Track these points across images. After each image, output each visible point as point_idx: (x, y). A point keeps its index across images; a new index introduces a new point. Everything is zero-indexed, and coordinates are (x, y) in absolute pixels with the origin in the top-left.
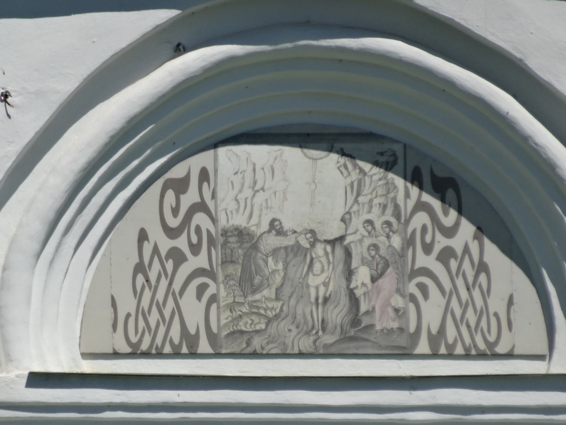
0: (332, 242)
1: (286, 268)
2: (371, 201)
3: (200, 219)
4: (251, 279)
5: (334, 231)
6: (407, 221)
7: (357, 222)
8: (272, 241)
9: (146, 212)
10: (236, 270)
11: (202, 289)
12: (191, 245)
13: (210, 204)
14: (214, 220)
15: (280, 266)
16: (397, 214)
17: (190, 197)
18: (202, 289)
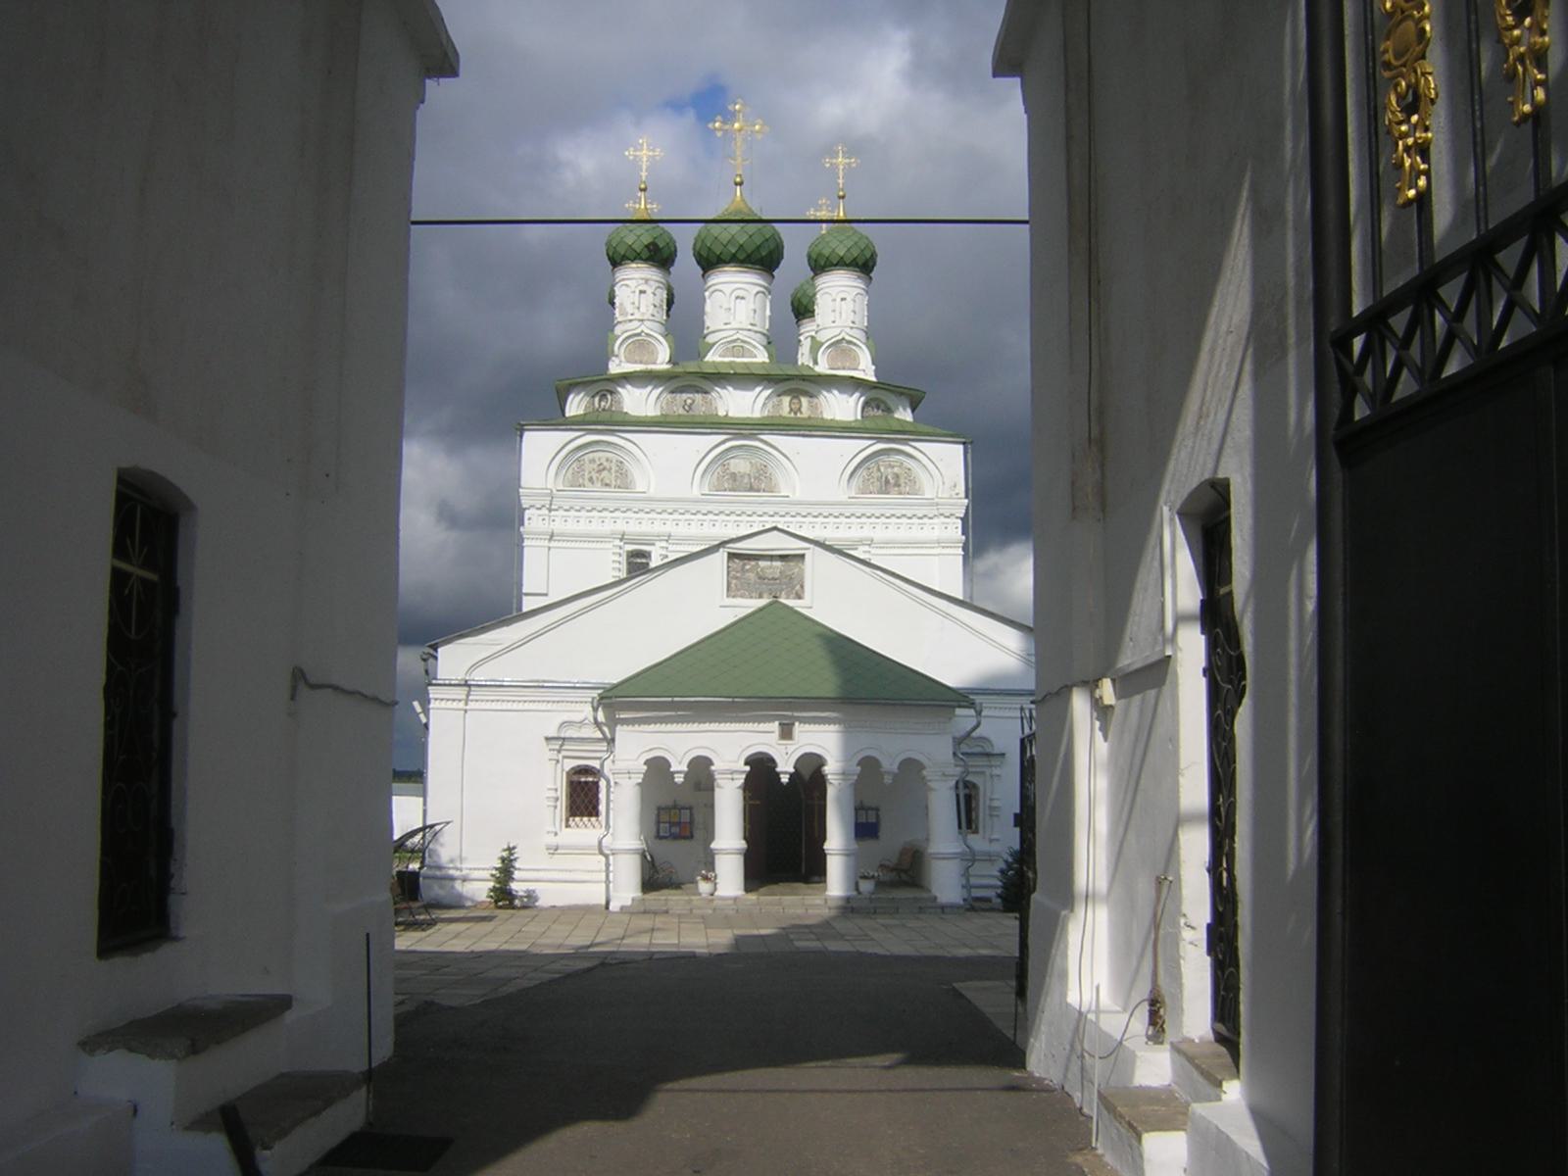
9: (719, 470)
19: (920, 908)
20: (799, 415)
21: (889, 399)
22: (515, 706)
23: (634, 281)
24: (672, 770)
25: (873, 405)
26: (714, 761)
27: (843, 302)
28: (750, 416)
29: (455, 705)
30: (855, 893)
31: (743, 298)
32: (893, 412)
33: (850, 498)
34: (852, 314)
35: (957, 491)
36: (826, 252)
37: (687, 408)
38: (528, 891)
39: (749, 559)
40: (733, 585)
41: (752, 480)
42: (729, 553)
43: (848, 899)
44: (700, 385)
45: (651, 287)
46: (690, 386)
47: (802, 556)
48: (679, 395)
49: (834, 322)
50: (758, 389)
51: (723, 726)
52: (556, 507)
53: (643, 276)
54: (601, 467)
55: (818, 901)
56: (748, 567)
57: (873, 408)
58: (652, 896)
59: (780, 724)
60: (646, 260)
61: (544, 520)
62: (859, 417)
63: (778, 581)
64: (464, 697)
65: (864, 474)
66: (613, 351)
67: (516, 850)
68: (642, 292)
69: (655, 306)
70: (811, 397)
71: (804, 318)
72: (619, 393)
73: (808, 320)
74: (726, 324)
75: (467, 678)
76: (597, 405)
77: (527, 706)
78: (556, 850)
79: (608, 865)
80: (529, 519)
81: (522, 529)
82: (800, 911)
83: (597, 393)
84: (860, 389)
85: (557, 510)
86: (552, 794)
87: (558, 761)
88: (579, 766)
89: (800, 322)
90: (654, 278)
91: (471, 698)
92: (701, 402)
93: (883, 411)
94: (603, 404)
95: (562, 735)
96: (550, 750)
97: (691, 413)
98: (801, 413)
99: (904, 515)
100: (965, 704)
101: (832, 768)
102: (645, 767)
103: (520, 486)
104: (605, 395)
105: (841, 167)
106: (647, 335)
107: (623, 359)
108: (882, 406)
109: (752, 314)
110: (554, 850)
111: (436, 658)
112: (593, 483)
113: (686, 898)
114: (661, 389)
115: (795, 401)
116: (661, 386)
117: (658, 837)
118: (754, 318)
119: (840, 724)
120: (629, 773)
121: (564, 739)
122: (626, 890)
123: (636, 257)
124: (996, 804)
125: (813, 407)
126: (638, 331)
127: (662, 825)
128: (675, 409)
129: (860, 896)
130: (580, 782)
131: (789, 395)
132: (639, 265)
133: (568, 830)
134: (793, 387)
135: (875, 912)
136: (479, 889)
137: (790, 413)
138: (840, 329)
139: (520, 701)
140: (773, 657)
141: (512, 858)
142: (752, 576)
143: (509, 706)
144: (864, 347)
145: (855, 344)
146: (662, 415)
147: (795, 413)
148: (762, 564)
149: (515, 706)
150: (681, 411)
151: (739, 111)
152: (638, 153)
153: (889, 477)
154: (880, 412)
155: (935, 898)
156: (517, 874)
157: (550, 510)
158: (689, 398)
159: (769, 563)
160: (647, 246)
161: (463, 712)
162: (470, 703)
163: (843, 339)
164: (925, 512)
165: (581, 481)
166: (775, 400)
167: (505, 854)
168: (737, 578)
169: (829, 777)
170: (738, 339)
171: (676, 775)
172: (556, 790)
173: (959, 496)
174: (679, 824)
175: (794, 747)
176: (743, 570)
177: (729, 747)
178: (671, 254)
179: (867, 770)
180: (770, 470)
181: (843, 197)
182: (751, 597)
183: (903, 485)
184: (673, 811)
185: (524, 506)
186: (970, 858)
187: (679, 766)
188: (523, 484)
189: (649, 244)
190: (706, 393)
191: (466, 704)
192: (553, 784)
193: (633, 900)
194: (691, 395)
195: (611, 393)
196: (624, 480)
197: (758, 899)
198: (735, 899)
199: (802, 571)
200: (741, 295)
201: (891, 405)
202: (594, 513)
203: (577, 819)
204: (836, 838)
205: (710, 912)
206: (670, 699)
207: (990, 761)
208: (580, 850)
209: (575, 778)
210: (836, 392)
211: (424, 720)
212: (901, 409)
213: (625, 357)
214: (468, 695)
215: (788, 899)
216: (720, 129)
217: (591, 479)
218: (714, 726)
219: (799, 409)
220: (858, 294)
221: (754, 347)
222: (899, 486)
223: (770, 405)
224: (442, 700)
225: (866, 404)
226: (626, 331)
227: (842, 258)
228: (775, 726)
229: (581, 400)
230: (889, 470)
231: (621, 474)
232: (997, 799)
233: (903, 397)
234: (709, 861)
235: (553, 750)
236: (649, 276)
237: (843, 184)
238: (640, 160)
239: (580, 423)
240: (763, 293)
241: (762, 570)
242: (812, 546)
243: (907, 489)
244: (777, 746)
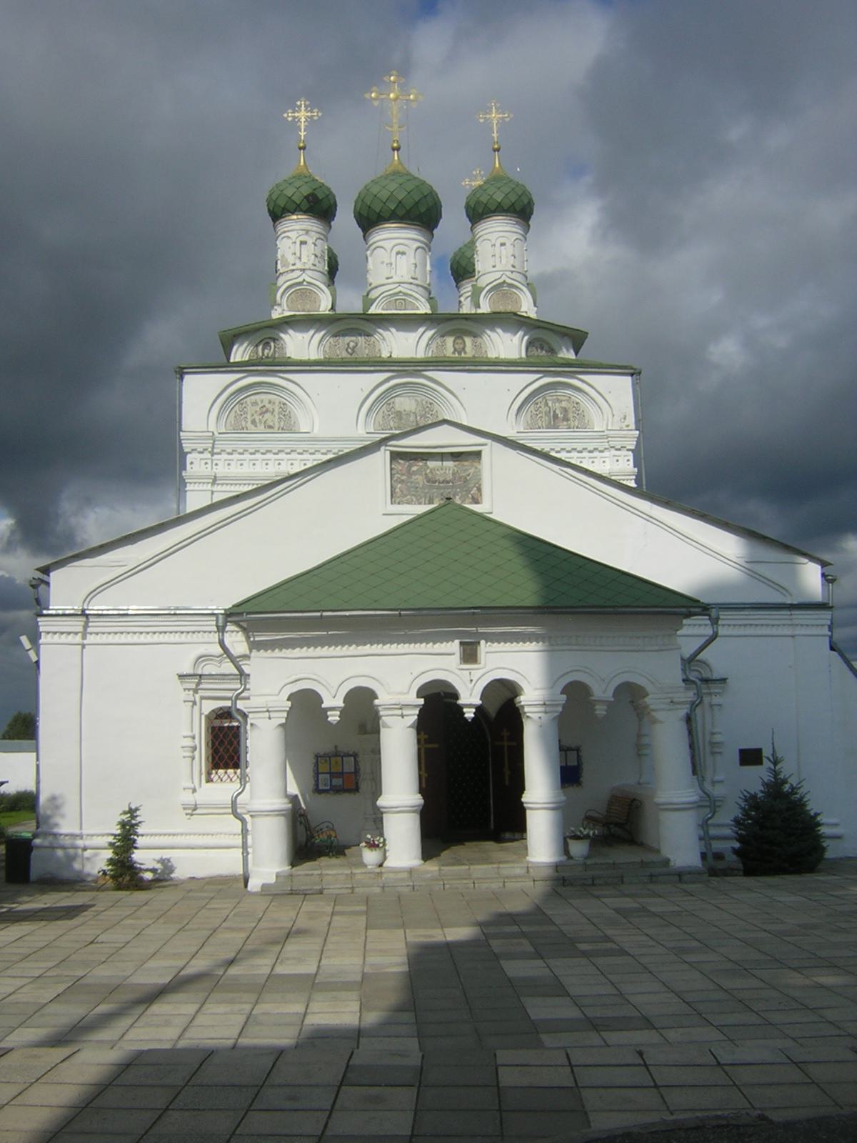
7: (418, 410)
8: (404, 413)
17: (391, 406)
19: (651, 876)
20: (463, 355)
22: (143, 639)
23: (295, 232)
24: (323, 706)
25: (537, 344)
26: (378, 693)
27: (503, 247)
28: (414, 356)
29: (70, 639)
30: (564, 858)
31: (403, 253)
32: (556, 353)
33: (518, 432)
34: (513, 258)
35: (626, 423)
36: (484, 199)
37: (349, 350)
38: (162, 861)
40: (397, 490)
41: (418, 418)
42: (392, 453)
43: (557, 867)
44: (362, 328)
45: (312, 237)
48: (341, 338)
49: (494, 267)
50: (421, 330)
51: (388, 648)
52: (219, 451)
53: (303, 227)
54: (264, 409)
55: (518, 870)
56: (414, 468)
58: (306, 868)
59: (461, 643)
60: (305, 212)
61: (206, 463)
62: (524, 355)
63: (451, 484)
64: (81, 629)
65: (532, 408)
66: (275, 301)
67: (138, 813)
68: (303, 243)
69: (316, 256)
70: (475, 337)
71: (463, 280)
72: (281, 338)
73: (467, 281)
74: (387, 278)
75: (85, 607)
76: (260, 354)
77: (156, 638)
78: (195, 809)
79: (245, 832)
80: (192, 463)
81: (184, 474)
82: (495, 886)
83: (261, 341)
84: (524, 328)
85: (219, 454)
86: (188, 742)
87: (194, 703)
88: (221, 708)
89: (459, 285)
90: (315, 229)
91: (89, 630)
93: (546, 351)
94: (266, 351)
95: (200, 672)
96: (185, 689)
97: (354, 355)
98: (465, 353)
99: (575, 449)
100: (696, 610)
101: (532, 697)
102: (289, 704)
103: (180, 430)
105: (495, 122)
106: (310, 283)
107: (286, 308)
108: (546, 347)
109: (413, 269)
110: (193, 809)
111: (48, 584)
112: (256, 426)
113: (348, 872)
116: (323, 330)
117: (317, 790)
118: (415, 272)
119: (543, 642)
120: (268, 711)
121: (200, 676)
122: (269, 862)
123: (297, 209)
124: (718, 738)
126: (300, 280)
127: (320, 776)
128: (338, 352)
129: (571, 862)
130: (224, 727)
131: (451, 335)
132: (300, 217)
133: (209, 785)
134: (458, 326)
135: (593, 884)
136: (98, 862)
137: (454, 353)
138: (502, 273)
139: (148, 633)
140: (444, 567)
141: (133, 822)
142: (420, 479)
143: (135, 639)
144: (525, 289)
145: (517, 287)
146: (325, 358)
147: (460, 353)
148: (431, 464)
149: (143, 639)
150: (344, 354)
151: (394, 82)
152: (296, 115)
153: (558, 412)
154: (544, 352)
155: (666, 862)
156: (140, 841)
157: (213, 454)
158: (353, 341)
159: (439, 463)
160: (306, 197)
161: (80, 646)
162: (88, 636)
163: (504, 282)
164: (595, 445)
165: (244, 423)
166: (439, 340)
167: (126, 817)
169: (526, 709)
170: (400, 292)
171: (329, 713)
172: (193, 738)
173: (630, 428)
174: (341, 774)
175: (479, 673)
176: (410, 474)
177: (398, 675)
178: (330, 207)
179: (574, 702)
180: (436, 407)
181: (498, 150)
182: (420, 504)
183: (572, 419)
184: (333, 760)
185: (186, 450)
186: (709, 804)
187: (333, 700)
188: (184, 428)
189: (309, 195)
190: (369, 335)
191: (84, 637)
192: (188, 729)
193: (278, 876)
194: (353, 338)
195: (274, 340)
196: (288, 425)
197: (440, 870)
198: (411, 871)
200: (401, 251)
201: (555, 346)
202: (258, 456)
203: (221, 772)
204: (539, 786)
205: (378, 890)
206: (319, 614)
207: (709, 688)
208: (214, 809)
209: (217, 723)
210: (499, 331)
211: (34, 659)
212: (564, 350)
213: (288, 306)
214: (86, 626)
215: (479, 870)
216: (376, 99)
217: (254, 422)
218: (377, 648)
219: (464, 349)
220: (517, 239)
221: (417, 299)
222: (568, 420)
223: (433, 346)
224: (55, 633)
225: (530, 344)
226: (287, 281)
227: (500, 203)
228: (454, 646)
229: (246, 349)
230: (557, 404)
232: (720, 733)
234: (377, 819)
235: (189, 690)
236: (309, 228)
237: (498, 137)
238: (299, 120)
239: (241, 367)
240: (423, 248)
241: (431, 472)
242: (489, 441)
244: (458, 672)
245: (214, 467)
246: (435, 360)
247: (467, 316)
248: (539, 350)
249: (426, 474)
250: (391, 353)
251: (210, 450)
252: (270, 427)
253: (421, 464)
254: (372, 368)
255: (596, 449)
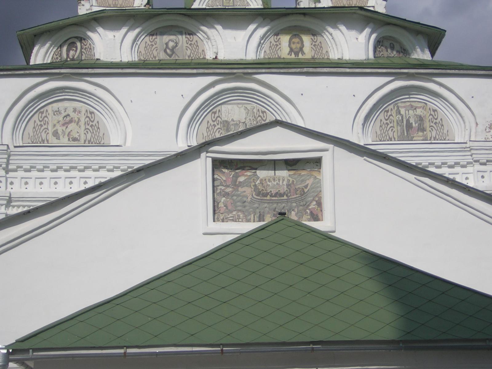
0: (243, 123)
1: (235, 127)
2: (250, 115)
3: (219, 119)
4: (228, 129)
5: (243, 121)
6: (257, 119)
7: (248, 119)
8: (232, 123)
9: (209, 118)
10: (225, 128)
11: (219, 131)
12: (217, 124)
13: (221, 116)
14: (221, 119)
15: (234, 127)
16: (255, 118)
17: (217, 115)
18: (219, 131)
20: (300, 56)
21: (405, 38)
28: (244, 58)
32: (409, 54)
37: (168, 51)
39: (243, 168)
40: (221, 205)
46: (172, 27)
47: (317, 162)
48: (158, 37)
50: (252, 27)
52: (14, 167)
56: (241, 179)
57: (386, 48)
62: (371, 56)
63: (285, 197)
65: (382, 117)
72: (89, 38)
76: (65, 56)
85: (15, 170)
92: (185, 45)
93: (397, 52)
94: (72, 53)
98: (303, 53)
104: (74, 43)
107: (94, 4)
108: (397, 47)
112: (58, 138)
114: (137, 31)
115: (296, 40)
125: (317, 46)
128: (155, 53)
131: (287, 33)
137: (290, 53)
142: (248, 191)
147: (297, 54)
148: (262, 174)
150: (162, 56)
153: (412, 120)
154: (395, 53)
157: (7, 171)
158: (172, 41)
159: (271, 173)
166: (272, 39)
168: (226, 195)
176: (236, 185)
182: (248, 221)
183: (428, 129)
190: (191, 33)
195: (81, 39)
196: (95, 137)
199: (318, 184)
202: (61, 173)
206: (122, 351)
212: (419, 50)
217: (56, 134)
219: (301, 49)
222: (423, 130)
223: (266, 46)
225: (378, 43)
230: (411, 112)
231: (92, 126)
233: (420, 37)
239: (43, 70)
241: (261, 183)
242: (330, 146)
243: (434, 133)
245: (9, 186)
246: (267, 61)
247: (305, 11)
248: (389, 50)
249: (255, 186)
250: (217, 54)
251: (4, 166)
252: (75, 139)
253: (249, 173)
254: (195, 71)
255: (457, 164)
